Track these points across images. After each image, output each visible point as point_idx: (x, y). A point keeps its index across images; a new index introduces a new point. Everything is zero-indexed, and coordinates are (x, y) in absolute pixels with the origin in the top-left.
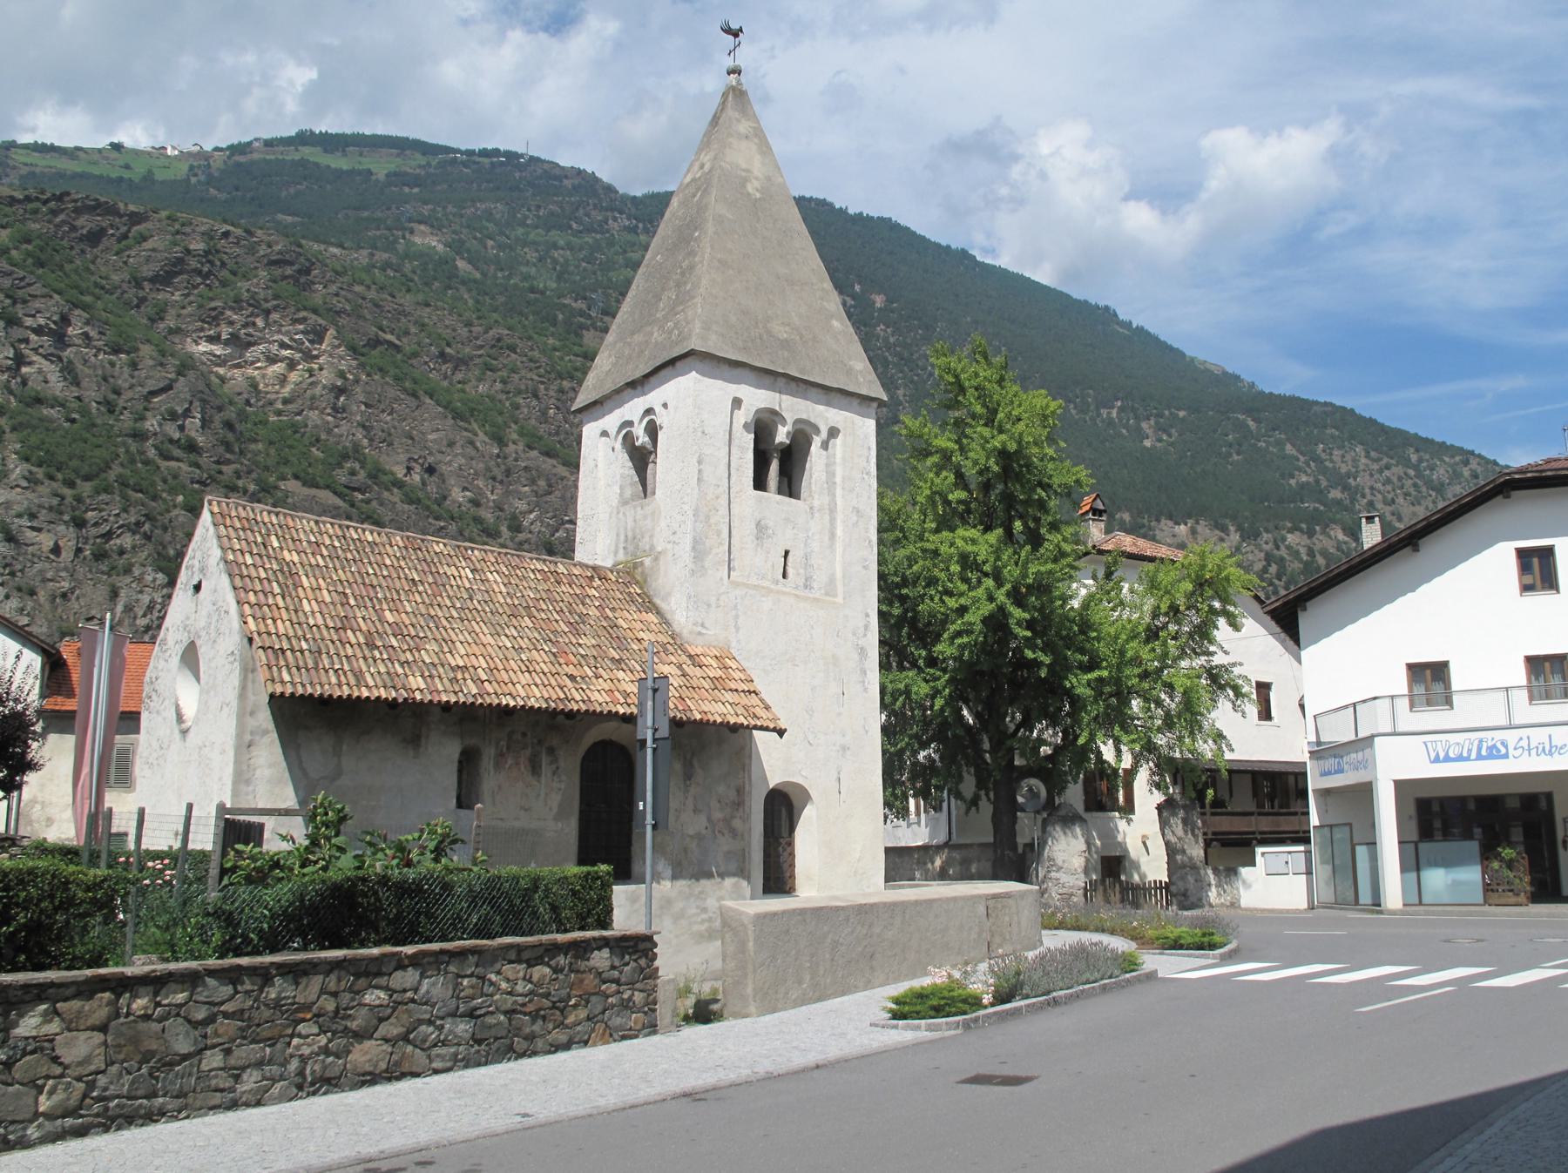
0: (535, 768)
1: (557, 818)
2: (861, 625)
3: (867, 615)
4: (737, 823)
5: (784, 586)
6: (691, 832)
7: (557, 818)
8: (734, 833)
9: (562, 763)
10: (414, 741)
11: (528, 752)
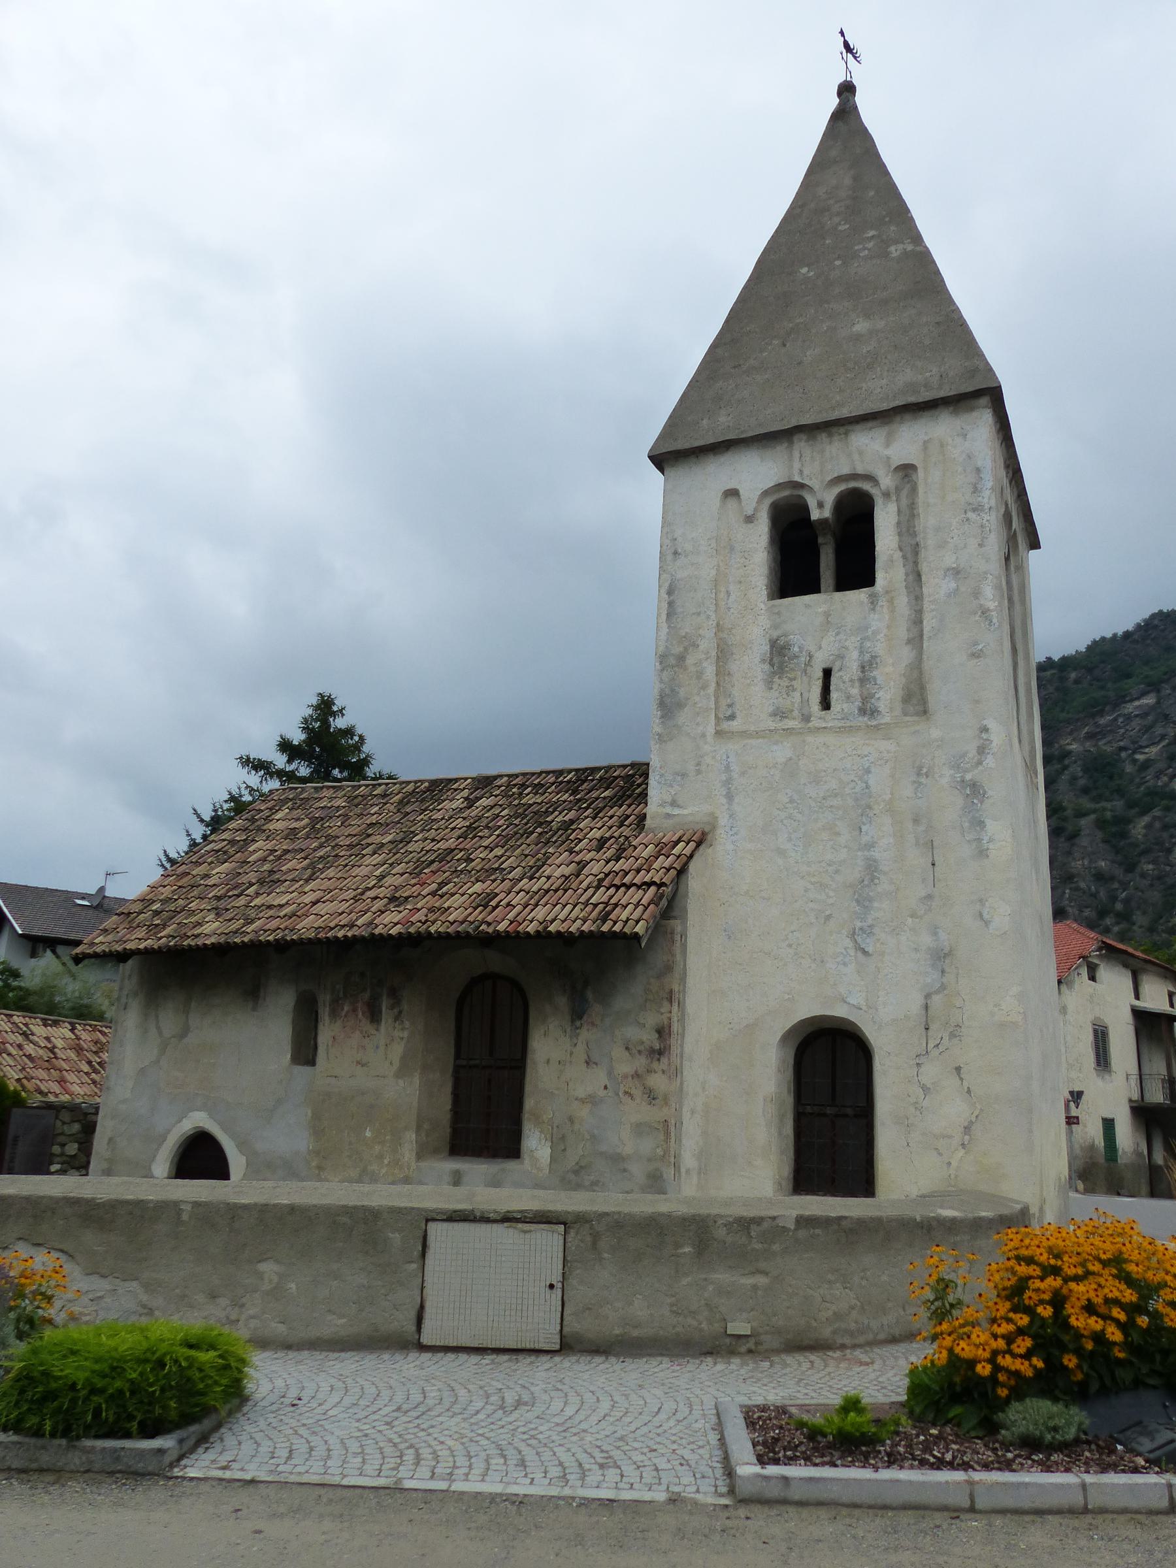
0: (374, 1016)
1: (399, 1075)
2: (971, 750)
3: (985, 729)
4: (657, 1081)
5: (831, 719)
6: (581, 1092)
7: (399, 1075)
8: (651, 1096)
9: (405, 1006)
10: (253, 994)
11: (366, 996)
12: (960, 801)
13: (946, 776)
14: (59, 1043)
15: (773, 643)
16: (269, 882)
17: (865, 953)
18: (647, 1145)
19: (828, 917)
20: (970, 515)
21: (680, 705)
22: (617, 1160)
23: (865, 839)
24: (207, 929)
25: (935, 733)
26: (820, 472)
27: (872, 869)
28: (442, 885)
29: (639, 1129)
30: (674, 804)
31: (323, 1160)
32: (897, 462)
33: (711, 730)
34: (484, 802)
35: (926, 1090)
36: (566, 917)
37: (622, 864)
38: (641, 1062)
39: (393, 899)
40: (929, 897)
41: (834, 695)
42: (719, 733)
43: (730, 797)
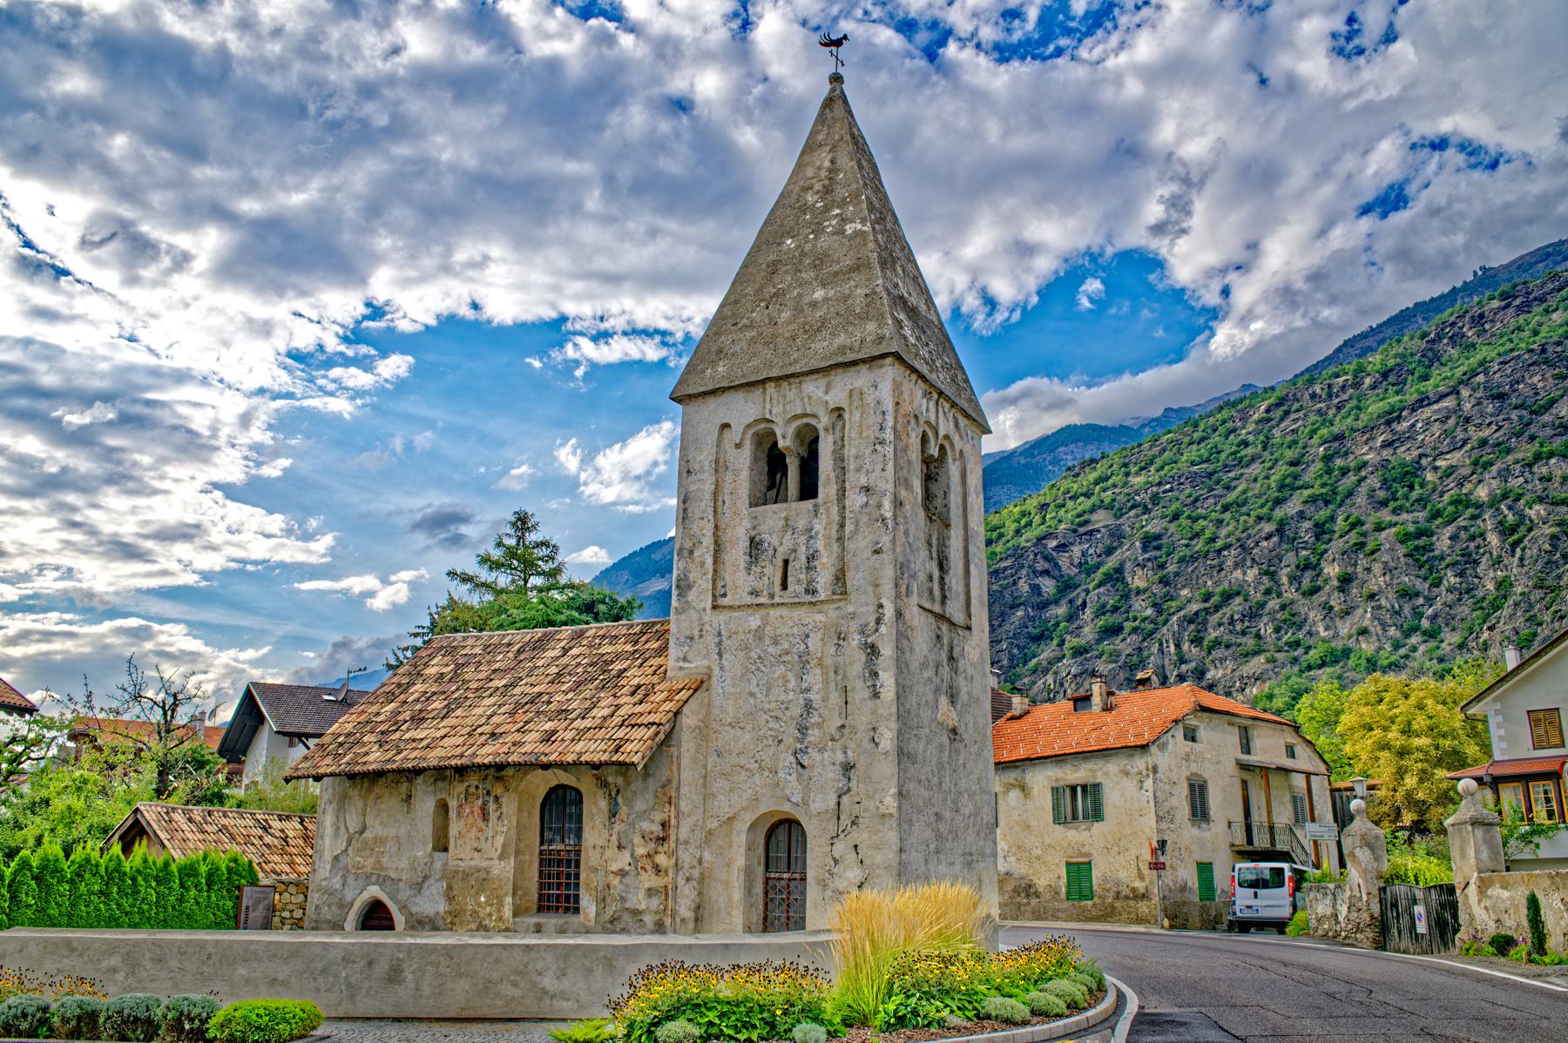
2: (872, 620)
3: (881, 606)
5: (787, 597)
6: (614, 867)
12: (863, 658)
13: (855, 640)
14: (291, 834)
15: (752, 540)
16: (418, 720)
17: (803, 767)
18: (655, 903)
19: (780, 742)
20: (878, 447)
21: (689, 587)
22: (636, 913)
23: (805, 685)
24: (371, 758)
25: (851, 609)
26: (782, 411)
27: (808, 706)
28: (527, 723)
29: (651, 892)
30: (685, 659)
31: (452, 921)
32: (832, 406)
33: (709, 606)
34: (575, 651)
35: (836, 862)
36: (594, 750)
37: (639, 709)
38: (652, 845)
39: (493, 734)
40: (843, 726)
41: (790, 579)
42: (714, 607)
43: (720, 654)
